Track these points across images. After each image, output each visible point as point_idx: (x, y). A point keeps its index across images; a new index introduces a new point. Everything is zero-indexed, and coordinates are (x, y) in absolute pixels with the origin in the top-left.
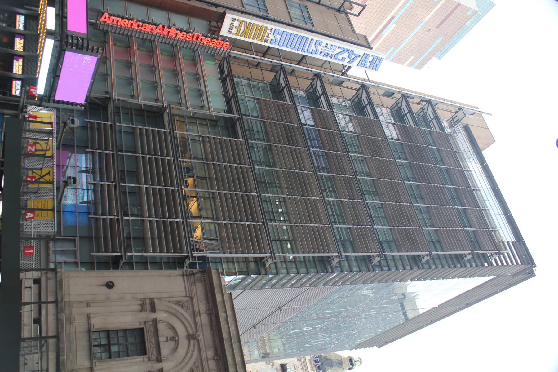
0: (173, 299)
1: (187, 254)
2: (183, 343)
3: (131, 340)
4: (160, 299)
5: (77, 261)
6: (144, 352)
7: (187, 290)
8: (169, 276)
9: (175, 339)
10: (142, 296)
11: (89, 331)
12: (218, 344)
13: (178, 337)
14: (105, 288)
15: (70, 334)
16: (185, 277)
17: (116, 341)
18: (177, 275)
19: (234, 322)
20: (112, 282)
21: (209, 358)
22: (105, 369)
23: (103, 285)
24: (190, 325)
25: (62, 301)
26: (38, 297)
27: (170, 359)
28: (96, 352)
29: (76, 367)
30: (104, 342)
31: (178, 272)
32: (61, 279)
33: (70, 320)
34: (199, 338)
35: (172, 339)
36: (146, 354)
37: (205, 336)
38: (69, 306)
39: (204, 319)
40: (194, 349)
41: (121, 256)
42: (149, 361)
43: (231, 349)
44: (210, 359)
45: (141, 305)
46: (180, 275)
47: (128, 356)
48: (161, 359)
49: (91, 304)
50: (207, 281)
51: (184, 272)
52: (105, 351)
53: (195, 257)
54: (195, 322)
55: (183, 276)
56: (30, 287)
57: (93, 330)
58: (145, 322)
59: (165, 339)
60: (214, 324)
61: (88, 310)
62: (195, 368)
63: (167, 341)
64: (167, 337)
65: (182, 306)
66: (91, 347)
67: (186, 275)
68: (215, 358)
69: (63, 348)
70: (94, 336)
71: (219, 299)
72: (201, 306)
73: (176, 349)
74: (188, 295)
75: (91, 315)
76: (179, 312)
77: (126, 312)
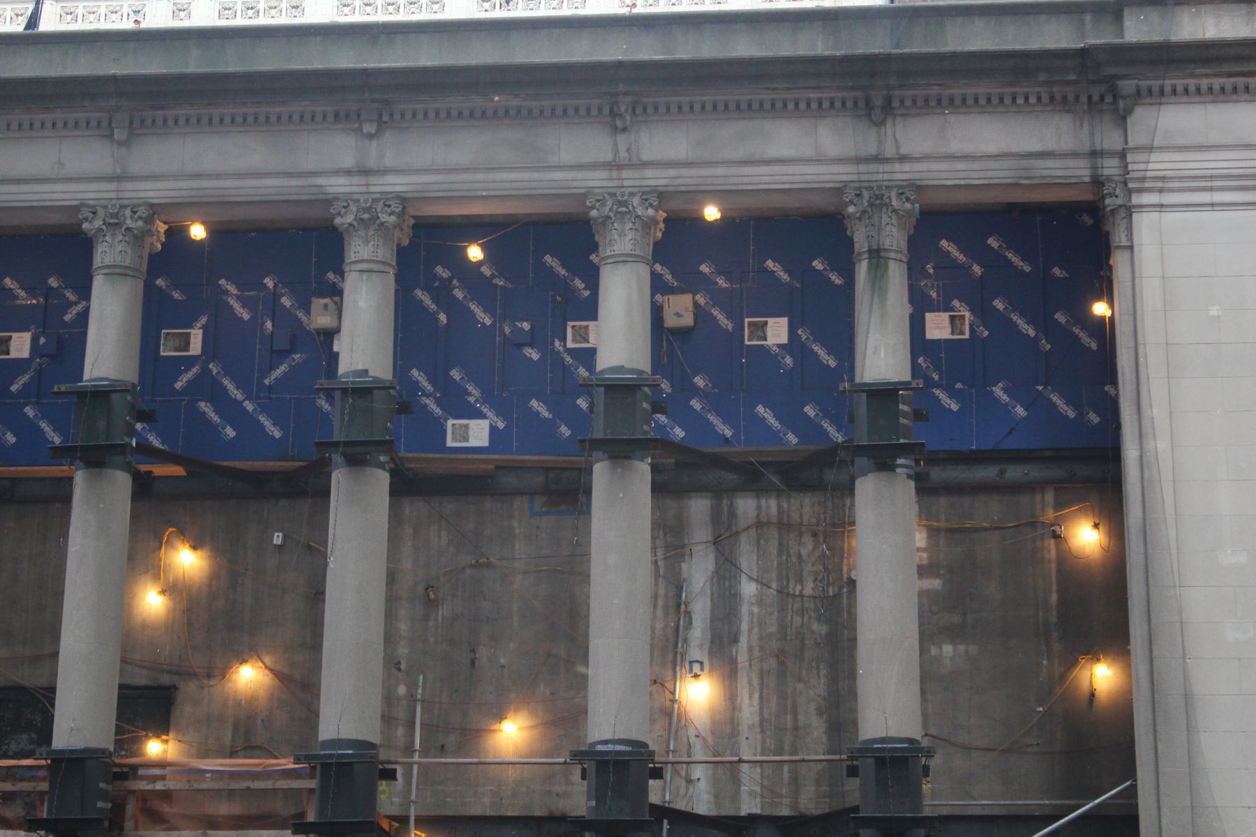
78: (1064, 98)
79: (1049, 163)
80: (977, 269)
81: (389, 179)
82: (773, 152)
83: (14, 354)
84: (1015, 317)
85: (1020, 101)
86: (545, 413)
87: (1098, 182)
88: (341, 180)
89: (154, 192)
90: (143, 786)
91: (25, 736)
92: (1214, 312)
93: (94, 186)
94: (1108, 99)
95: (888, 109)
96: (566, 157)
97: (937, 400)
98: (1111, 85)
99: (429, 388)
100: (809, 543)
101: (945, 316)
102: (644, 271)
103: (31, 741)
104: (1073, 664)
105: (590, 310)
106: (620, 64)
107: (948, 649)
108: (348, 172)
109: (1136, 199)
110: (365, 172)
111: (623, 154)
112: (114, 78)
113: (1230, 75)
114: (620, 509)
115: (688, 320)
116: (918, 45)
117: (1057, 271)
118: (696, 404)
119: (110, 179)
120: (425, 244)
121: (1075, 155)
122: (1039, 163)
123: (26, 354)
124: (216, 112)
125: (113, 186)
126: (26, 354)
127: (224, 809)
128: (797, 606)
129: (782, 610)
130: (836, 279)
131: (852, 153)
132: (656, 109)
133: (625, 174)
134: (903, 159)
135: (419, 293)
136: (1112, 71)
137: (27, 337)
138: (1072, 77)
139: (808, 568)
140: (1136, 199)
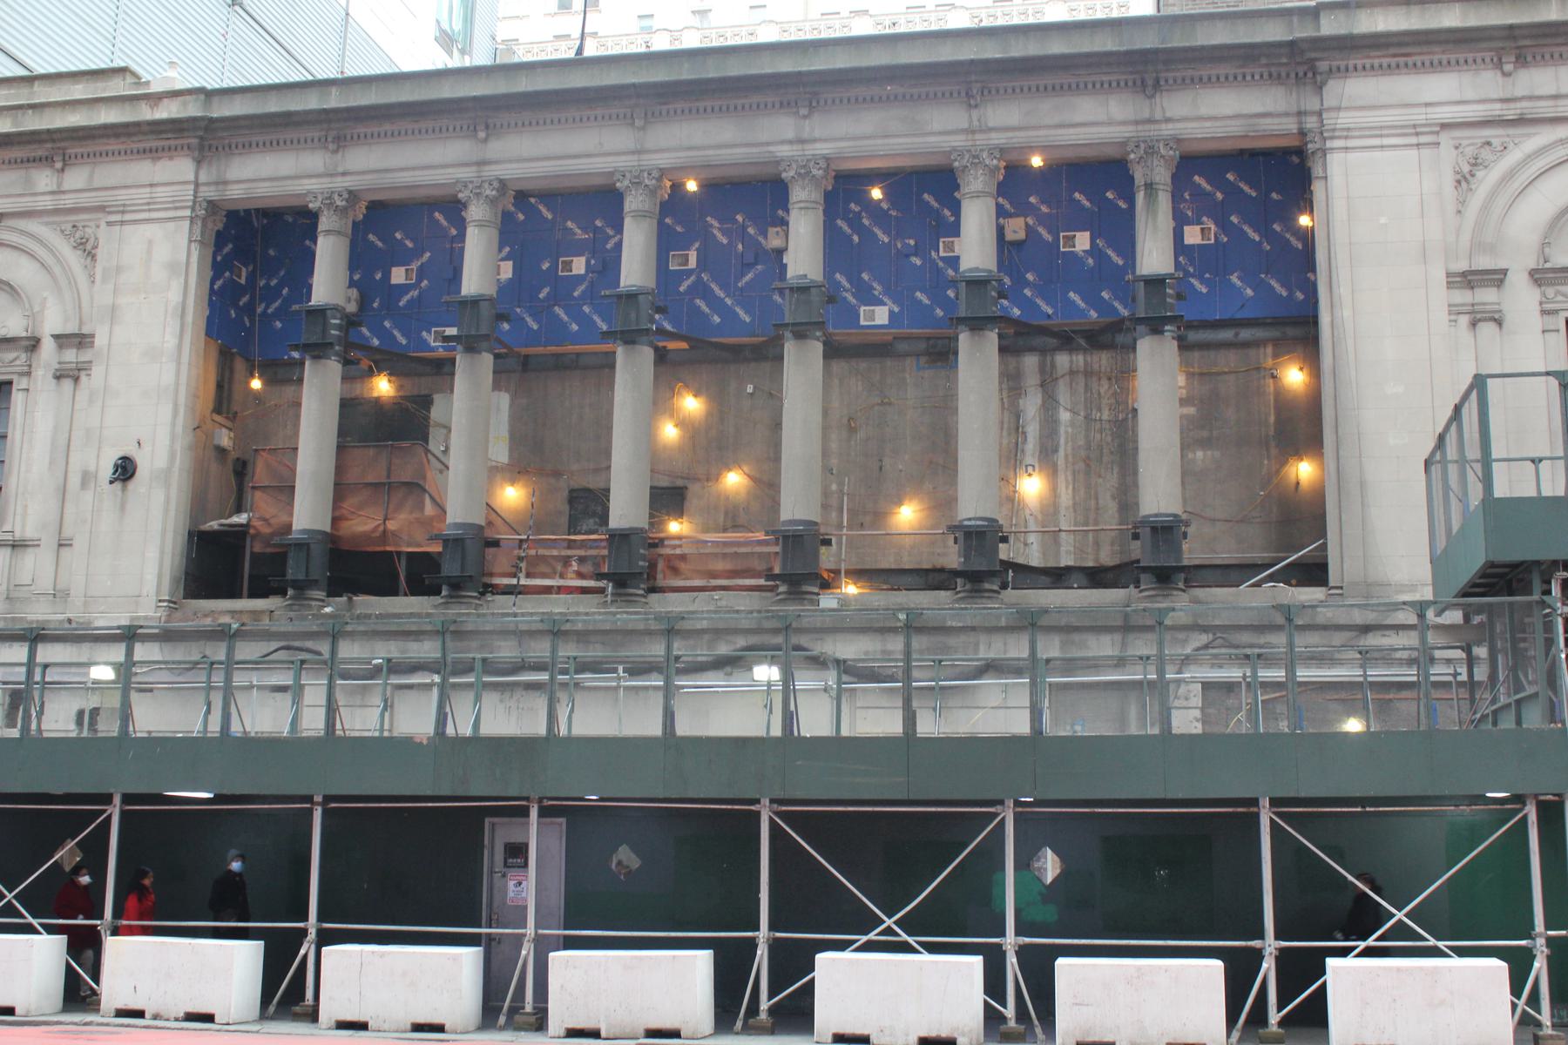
21: (55, 188)
27: (36, 309)
36: (10, 383)
40: (23, 232)
42: (29, 374)
43: (47, 111)
44: (59, 184)
48: (28, 338)
68: (59, 165)
78: (1279, 76)
79: (1269, 120)
80: (1219, 196)
81: (818, 145)
82: (1078, 119)
83: (575, 272)
84: (1246, 228)
85: (1249, 78)
86: (926, 301)
87: (1302, 133)
88: (786, 147)
89: (663, 160)
90: (668, 551)
91: (591, 521)
92: (1383, 220)
93: (623, 158)
94: (1310, 75)
95: (1157, 85)
96: (936, 127)
97: (1192, 285)
98: (1311, 65)
99: (848, 286)
100: (1105, 383)
101: (1198, 228)
102: (991, 203)
104: (1284, 463)
105: (955, 230)
106: (972, 62)
107: (1200, 454)
108: (790, 142)
109: (1329, 144)
110: (802, 141)
111: (976, 123)
112: (634, 85)
113: (1395, 56)
114: (978, 360)
115: (1022, 235)
116: (1177, 41)
117: (1274, 196)
118: (1027, 292)
119: (633, 153)
120: (843, 188)
121: (1287, 114)
122: (1262, 121)
123: (582, 271)
124: (701, 105)
125: (636, 157)
126: (582, 271)
127: (720, 566)
128: (1098, 426)
129: (1087, 430)
131: (1132, 117)
133: (977, 136)
134: (1168, 120)
135: (839, 222)
136: (1313, 55)
137: (583, 259)
138: (1284, 60)
139: (1105, 401)
140: (1329, 144)
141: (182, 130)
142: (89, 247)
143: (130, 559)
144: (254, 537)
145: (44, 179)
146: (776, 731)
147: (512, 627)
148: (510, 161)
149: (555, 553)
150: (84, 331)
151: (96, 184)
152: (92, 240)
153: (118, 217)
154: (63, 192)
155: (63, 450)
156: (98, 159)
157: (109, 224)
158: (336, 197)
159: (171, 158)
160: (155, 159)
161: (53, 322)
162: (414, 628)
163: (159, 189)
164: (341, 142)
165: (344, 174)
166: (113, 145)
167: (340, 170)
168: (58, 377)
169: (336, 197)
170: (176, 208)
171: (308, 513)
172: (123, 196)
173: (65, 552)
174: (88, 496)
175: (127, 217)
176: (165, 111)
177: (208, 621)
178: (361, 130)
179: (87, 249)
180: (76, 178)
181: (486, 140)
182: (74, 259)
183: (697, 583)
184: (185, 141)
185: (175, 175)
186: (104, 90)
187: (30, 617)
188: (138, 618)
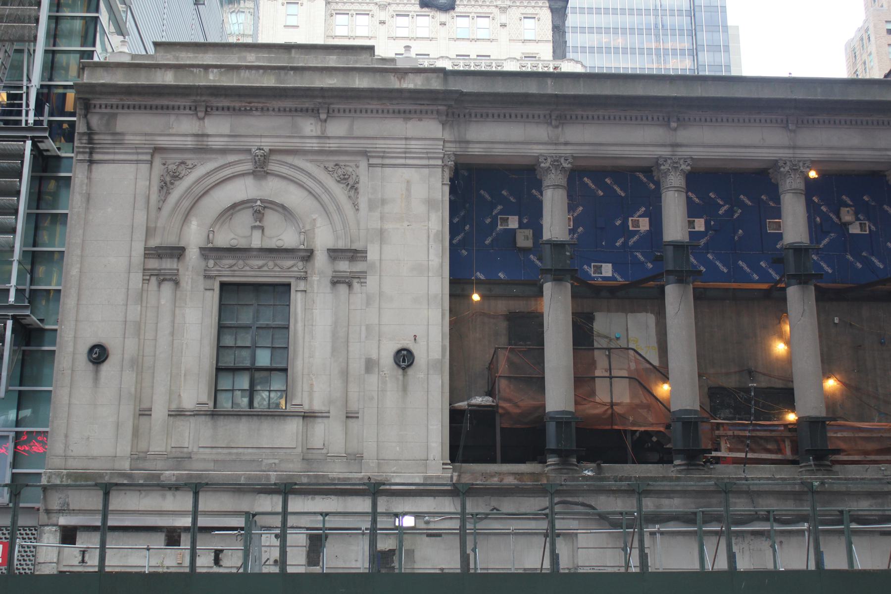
0: (154, 197)
1: (29, 143)
2: (272, 189)
3: (246, 317)
4: (149, 232)
5: (12, 435)
6: (283, 289)
7: (134, 157)
8: (88, 198)
9: (260, 209)
10: (137, 278)
11: (214, 414)
12: (288, 104)
13: (255, 201)
14: (105, 367)
15: (215, 461)
16: (96, 157)
17: (245, 353)
18: (89, 178)
19: (235, 50)
20: (92, 350)
21: (319, 133)
22: (312, 384)
23: (97, 372)
24: (229, 164)
25: (129, 476)
26: (116, 533)
28: (265, 403)
29: (299, 450)
30: (243, 382)
31: (79, 175)
32: (69, 476)
33: (181, 459)
34: (267, 149)
35: (259, 215)
36: (288, 285)
37: (263, 131)
38: (145, 459)
39: (218, 128)
40: (292, 166)
41: (14, 318)
42: (305, 278)
43: (307, 74)
44: (323, 131)
45: (160, 284)
46: (90, 170)
47: (287, 328)
48: (305, 250)
49: (145, 405)
50: (114, 101)
51: (80, 157)
52: (268, 381)
53: (35, 122)
54: (224, 151)
55: (91, 162)
56: (83, 553)
57: (211, 404)
58: (207, 277)
59: (257, 234)
60: (237, 105)
61: (159, 412)
62: (340, 172)
63: (262, 229)
64: (254, 228)
65: (176, 177)
66: (252, 414)
67: (91, 153)
68: (323, 116)
69: (249, 477)
70: (225, 404)
71: (168, 78)
72: (182, 128)
73: (284, 210)
74: (148, 157)
75: (174, 407)
76: (190, 188)
77: (173, 322)
83: (697, 229)
91: (727, 411)
93: (781, 151)
103: (731, 413)
112: (795, 100)
119: (789, 148)
123: (703, 229)
125: (791, 151)
126: (703, 229)
127: (870, 446)
130: (771, 204)
131: (453, 140)
132: (516, 116)
141: (436, 99)
142: (351, 182)
143: (412, 433)
144: (501, 415)
145: (309, 127)
146: (812, 566)
147: (745, 488)
148: (698, 146)
149: (747, 434)
150: (356, 246)
151: (357, 133)
152: (354, 177)
153: (379, 161)
154: (329, 138)
155: (340, 342)
156: (358, 114)
157: (370, 165)
158: (562, 160)
159: (420, 120)
160: (407, 119)
161: (323, 238)
162: (667, 488)
163: (413, 142)
164: (562, 120)
165: (566, 144)
166: (374, 105)
167: (562, 140)
168: (335, 282)
169: (562, 160)
170: (429, 158)
171: (558, 397)
172: (381, 144)
173: (353, 424)
174: (373, 380)
175: (387, 161)
176: (411, 83)
177: (495, 480)
178: (579, 112)
179: (352, 186)
180: (337, 128)
181: (675, 130)
182: (339, 191)
183: (857, 458)
184: (435, 108)
185: (428, 132)
186: (356, 62)
187: (331, 475)
188: (431, 477)
